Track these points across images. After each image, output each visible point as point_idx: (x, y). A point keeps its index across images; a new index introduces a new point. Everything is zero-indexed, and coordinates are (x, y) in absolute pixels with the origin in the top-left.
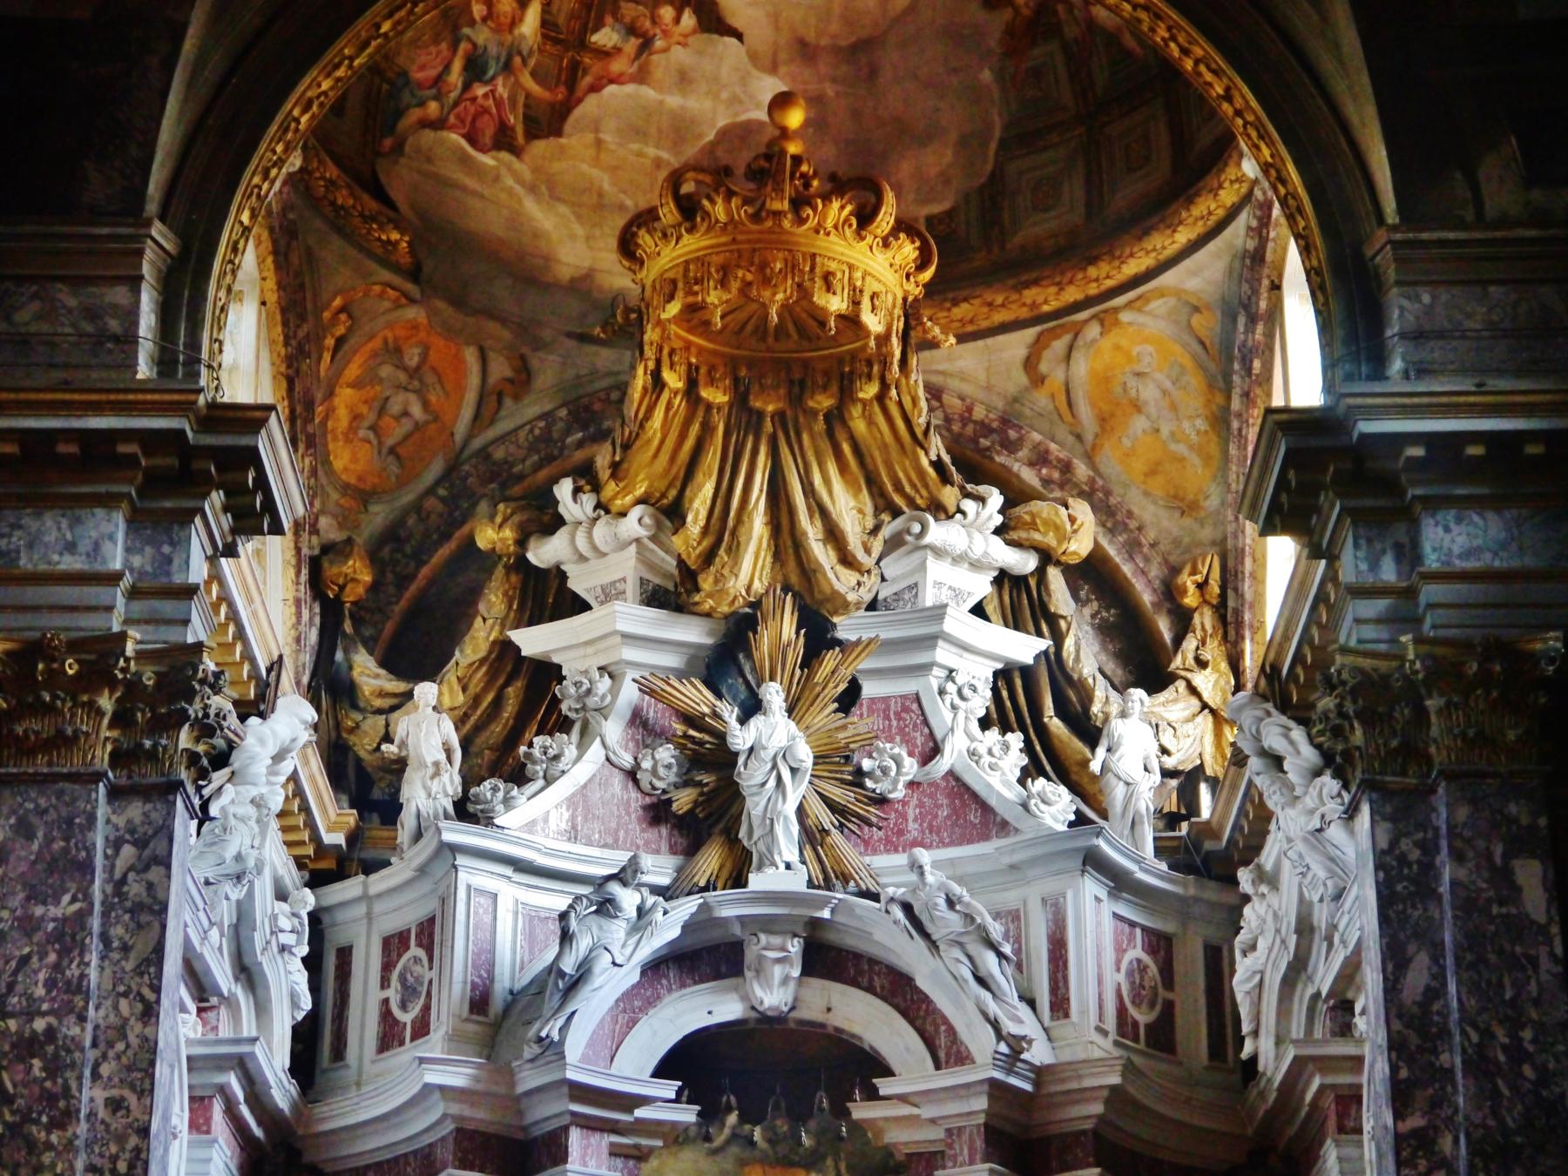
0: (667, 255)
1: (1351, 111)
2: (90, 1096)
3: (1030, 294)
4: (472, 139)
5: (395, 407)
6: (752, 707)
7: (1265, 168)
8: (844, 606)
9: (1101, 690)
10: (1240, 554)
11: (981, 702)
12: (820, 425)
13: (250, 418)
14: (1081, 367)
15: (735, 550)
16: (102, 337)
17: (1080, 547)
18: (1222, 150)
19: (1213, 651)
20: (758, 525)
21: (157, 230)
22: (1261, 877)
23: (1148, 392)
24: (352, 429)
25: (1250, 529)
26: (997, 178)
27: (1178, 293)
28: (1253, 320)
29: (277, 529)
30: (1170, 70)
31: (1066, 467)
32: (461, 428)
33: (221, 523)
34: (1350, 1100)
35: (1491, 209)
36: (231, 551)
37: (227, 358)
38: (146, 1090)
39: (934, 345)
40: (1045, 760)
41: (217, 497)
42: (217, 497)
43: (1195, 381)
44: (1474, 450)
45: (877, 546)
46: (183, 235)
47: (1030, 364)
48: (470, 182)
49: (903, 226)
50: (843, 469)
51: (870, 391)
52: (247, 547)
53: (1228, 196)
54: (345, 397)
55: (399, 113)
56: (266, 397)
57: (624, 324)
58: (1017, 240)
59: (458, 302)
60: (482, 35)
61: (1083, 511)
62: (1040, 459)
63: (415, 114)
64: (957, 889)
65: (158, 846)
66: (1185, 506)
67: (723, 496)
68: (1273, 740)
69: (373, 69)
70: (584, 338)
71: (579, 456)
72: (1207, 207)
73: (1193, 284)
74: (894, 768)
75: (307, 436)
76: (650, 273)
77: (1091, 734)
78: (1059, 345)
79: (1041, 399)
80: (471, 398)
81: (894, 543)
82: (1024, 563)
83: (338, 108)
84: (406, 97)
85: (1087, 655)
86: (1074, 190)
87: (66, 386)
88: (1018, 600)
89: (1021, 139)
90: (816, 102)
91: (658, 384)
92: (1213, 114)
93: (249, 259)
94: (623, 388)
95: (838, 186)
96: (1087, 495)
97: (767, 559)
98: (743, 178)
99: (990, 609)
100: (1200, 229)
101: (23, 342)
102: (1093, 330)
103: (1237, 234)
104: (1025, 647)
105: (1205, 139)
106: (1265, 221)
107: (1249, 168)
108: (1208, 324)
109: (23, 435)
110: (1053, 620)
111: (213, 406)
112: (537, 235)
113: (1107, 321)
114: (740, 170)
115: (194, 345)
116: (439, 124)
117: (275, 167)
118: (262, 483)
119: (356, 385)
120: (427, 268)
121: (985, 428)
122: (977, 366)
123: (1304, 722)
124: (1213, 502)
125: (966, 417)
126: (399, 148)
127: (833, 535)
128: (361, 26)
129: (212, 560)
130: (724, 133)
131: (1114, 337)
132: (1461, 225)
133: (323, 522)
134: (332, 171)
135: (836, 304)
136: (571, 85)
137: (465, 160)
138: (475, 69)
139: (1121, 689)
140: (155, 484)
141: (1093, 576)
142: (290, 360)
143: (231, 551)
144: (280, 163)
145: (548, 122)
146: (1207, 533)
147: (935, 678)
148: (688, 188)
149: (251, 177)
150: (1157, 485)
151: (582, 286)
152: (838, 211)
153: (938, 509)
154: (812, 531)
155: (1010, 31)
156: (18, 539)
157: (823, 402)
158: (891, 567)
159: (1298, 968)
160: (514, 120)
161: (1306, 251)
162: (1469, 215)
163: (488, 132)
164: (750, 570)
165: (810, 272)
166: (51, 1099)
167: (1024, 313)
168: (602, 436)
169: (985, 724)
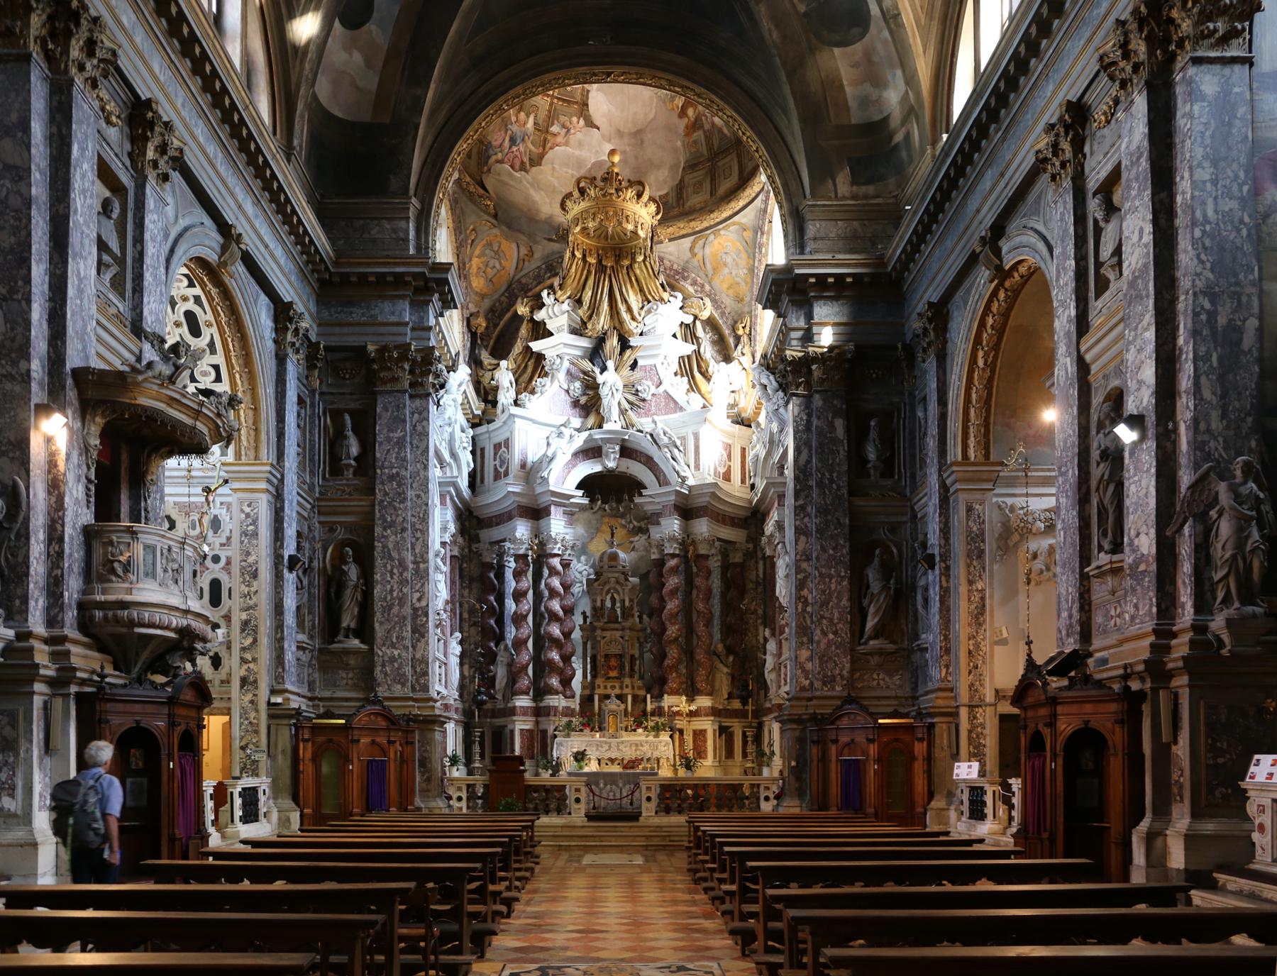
0: (575, 209)
1: (797, 157)
2: (410, 494)
3: (693, 224)
4: (512, 167)
5: (491, 265)
6: (604, 369)
7: (768, 177)
8: (632, 334)
9: (712, 362)
10: (756, 316)
11: (675, 367)
12: (625, 271)
13: (446, 267)
14: (708, 251)
15: (598, 315)
16: (399, 239)
17: (705, 315)
18: (754, 173)
19: (747, 350)
20: (605, 306)
21: (414, 200)
22: (758, 425)
23: (729, 260)
24: (478, 273)
25: (760, 307)
26: (682, 181)
27: (739, 224)
28: (763, 233)
29: (456, 307)
30: (738, 142)
31: (703, 286)
32: (512, 273)
33: (438, 305)
34: (781, 497)
35: (840, 195)
36: (442, 315)
37: (438, 246)
38: (426, 492)
39: (661, 242)
40: (693, 387)
41: (437, 296)
42: (437, 296)
43: (744, 255)
44: (831, 280)
45: (643, 313)
46: (422, 203)
47: (692, 249)
48: (512, 183)
49: (651, 199)
50: (632, 286)
51: (640, 258)
52: (447, 313)
53: (757, 189)
54: (476, 262)
55: (489, 157)
56: (450, 261)
57: (562, 235)
58: (688, 205)
59: (509, 227)
60: (515, 128)
61: (707, 301)
62: (694, 283)
63: (494, 158)
64: (667, 429)
65: (425, 414)
66: (739, 300)
67: (594, 295)
68: (764, 381)
69: (480, 141)
70: (550, 240)
71: (549, 282)
72: (750, 192)
73: (744, 221)
74: (647, 389)
75: (464, 275)
76: (570, 216)
77: (707, 378)
78: (701, 243)
79: (695, 261)
80: (515, 261)
81: (649, 312)
82: (689, 319)
83: (469, 156)
84: (491, 152)
85: (708, 351)
86: (707, 186)
87: (388, 257)
88: (688, 332)
89: (691, 166)
90: (623, 153)
91: (573, 255)
92: (752, 157)
93: (443, 211)
94: (562, 258)
95: (631, 184)
96: (709, 296)
97: (608, 317)
98: (602, 185)
99: (678, 335)
100: (747, 200)
101: (374, 241)
102: (712, 237)
103: (758, 202)
104: (689, 349)
105: (750, 167)
106: (767, 198)
107: (763, 178)
108: (748, 235)
109: (378, 275)
110: (697, 338)
111: (434, 263)
112: (534, 202)
113: (716, 234)
114: (599, 178)
115: (427, 242)
116: (501, 162)
117: (451, 177)
118: (450, 291)
119: (478, 257)
120: (500, 214)
121: (677, 272)
122: (673, 250)
123: (773, 373)
124: (748, 299)
125: (671, 269)
126: (489, 170)
127: (629, 309)
128: (475, 124)
129: (436, 318)
130: (594, 164)
131: (719, 239)
132: (830, 199)
133: (471, 305)
134: (468, 179)
135: (630, 227)
136: (544, 148)
137: (511, 175)
138: (513, 141)
139: (717, 362)
140: (417, 291)
141: (711, 324)
142: (457, 248)
143: (442, 315)
144: (451, 175)
145: (536, 161)
146: (746, 309)
147: (661, 358)
148: (582, 185)
149: (442, 181)
150: (731, 292)
151: (549, 221)
152: (630, 193)
153: (662, 300)
154: (622, 308)
155: (687, 127)
156: (377, 311)
157: (626, 263)
158: (648, 320)
159: (769, 454)
160: (526, 160)
161: (781, 208)
162: (833, 195)
163: (517, 167)
164: (603, 321)
165: (622, 216)
166: (400, 494)
167: (690, 231)
168: (556, 275)
169: (676, 374)
